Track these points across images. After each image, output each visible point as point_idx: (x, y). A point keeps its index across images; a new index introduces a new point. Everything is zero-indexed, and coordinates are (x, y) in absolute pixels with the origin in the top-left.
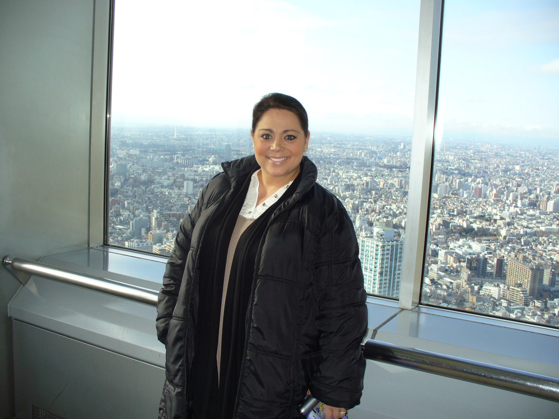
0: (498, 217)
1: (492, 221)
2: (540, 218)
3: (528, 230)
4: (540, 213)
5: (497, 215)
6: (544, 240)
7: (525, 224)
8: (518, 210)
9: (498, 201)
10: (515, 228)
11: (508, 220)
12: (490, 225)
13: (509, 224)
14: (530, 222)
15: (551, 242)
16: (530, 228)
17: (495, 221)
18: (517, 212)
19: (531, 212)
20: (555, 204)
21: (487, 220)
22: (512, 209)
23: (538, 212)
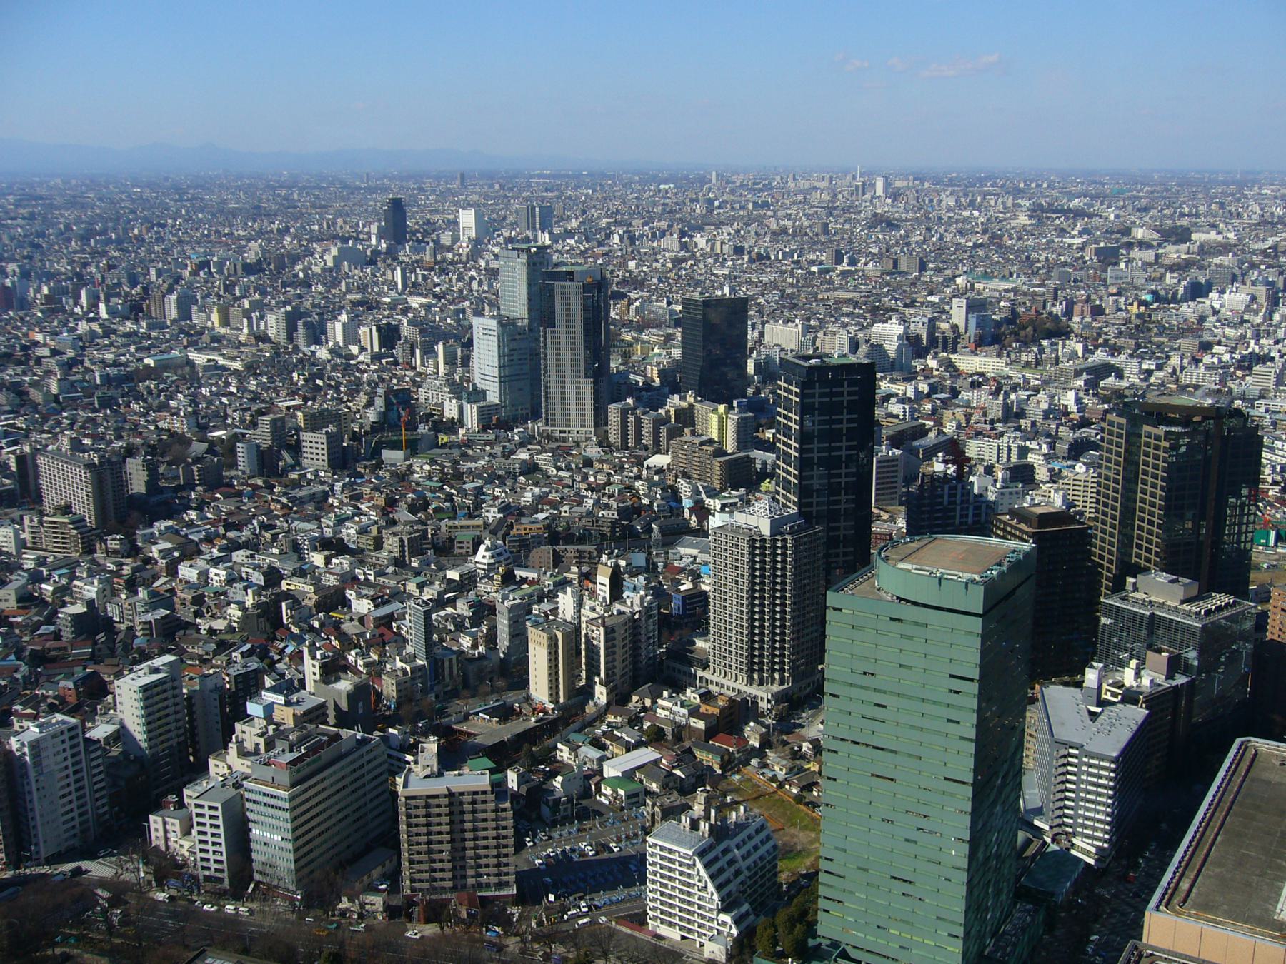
0: (46, 352)
1: (32, 363)
2: (149, 338)
3: (113, 371)
4: (150, 327)
5: (45, 345)
6: (148, 387)
7: (110, 357)
8: (95, 326)
9: (53, 311)
10: (88, 370)
11: (70, 353)
12: (24, 373)
13: (70, 365)
14: (122, 351)
15: (163, 390)
16: (120, 365)
17: (39, 361)
18: (92, 332)
19: (130, 326)
20: (178, 299)
21: (19, 363)
22: (83, 327)
23: (144, 324)
